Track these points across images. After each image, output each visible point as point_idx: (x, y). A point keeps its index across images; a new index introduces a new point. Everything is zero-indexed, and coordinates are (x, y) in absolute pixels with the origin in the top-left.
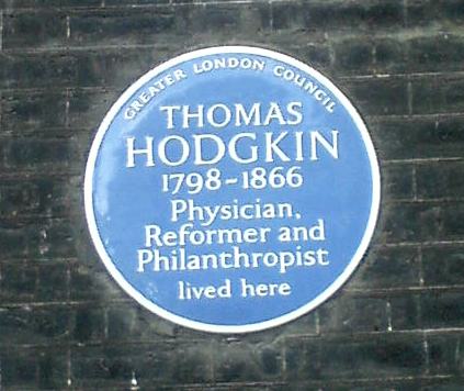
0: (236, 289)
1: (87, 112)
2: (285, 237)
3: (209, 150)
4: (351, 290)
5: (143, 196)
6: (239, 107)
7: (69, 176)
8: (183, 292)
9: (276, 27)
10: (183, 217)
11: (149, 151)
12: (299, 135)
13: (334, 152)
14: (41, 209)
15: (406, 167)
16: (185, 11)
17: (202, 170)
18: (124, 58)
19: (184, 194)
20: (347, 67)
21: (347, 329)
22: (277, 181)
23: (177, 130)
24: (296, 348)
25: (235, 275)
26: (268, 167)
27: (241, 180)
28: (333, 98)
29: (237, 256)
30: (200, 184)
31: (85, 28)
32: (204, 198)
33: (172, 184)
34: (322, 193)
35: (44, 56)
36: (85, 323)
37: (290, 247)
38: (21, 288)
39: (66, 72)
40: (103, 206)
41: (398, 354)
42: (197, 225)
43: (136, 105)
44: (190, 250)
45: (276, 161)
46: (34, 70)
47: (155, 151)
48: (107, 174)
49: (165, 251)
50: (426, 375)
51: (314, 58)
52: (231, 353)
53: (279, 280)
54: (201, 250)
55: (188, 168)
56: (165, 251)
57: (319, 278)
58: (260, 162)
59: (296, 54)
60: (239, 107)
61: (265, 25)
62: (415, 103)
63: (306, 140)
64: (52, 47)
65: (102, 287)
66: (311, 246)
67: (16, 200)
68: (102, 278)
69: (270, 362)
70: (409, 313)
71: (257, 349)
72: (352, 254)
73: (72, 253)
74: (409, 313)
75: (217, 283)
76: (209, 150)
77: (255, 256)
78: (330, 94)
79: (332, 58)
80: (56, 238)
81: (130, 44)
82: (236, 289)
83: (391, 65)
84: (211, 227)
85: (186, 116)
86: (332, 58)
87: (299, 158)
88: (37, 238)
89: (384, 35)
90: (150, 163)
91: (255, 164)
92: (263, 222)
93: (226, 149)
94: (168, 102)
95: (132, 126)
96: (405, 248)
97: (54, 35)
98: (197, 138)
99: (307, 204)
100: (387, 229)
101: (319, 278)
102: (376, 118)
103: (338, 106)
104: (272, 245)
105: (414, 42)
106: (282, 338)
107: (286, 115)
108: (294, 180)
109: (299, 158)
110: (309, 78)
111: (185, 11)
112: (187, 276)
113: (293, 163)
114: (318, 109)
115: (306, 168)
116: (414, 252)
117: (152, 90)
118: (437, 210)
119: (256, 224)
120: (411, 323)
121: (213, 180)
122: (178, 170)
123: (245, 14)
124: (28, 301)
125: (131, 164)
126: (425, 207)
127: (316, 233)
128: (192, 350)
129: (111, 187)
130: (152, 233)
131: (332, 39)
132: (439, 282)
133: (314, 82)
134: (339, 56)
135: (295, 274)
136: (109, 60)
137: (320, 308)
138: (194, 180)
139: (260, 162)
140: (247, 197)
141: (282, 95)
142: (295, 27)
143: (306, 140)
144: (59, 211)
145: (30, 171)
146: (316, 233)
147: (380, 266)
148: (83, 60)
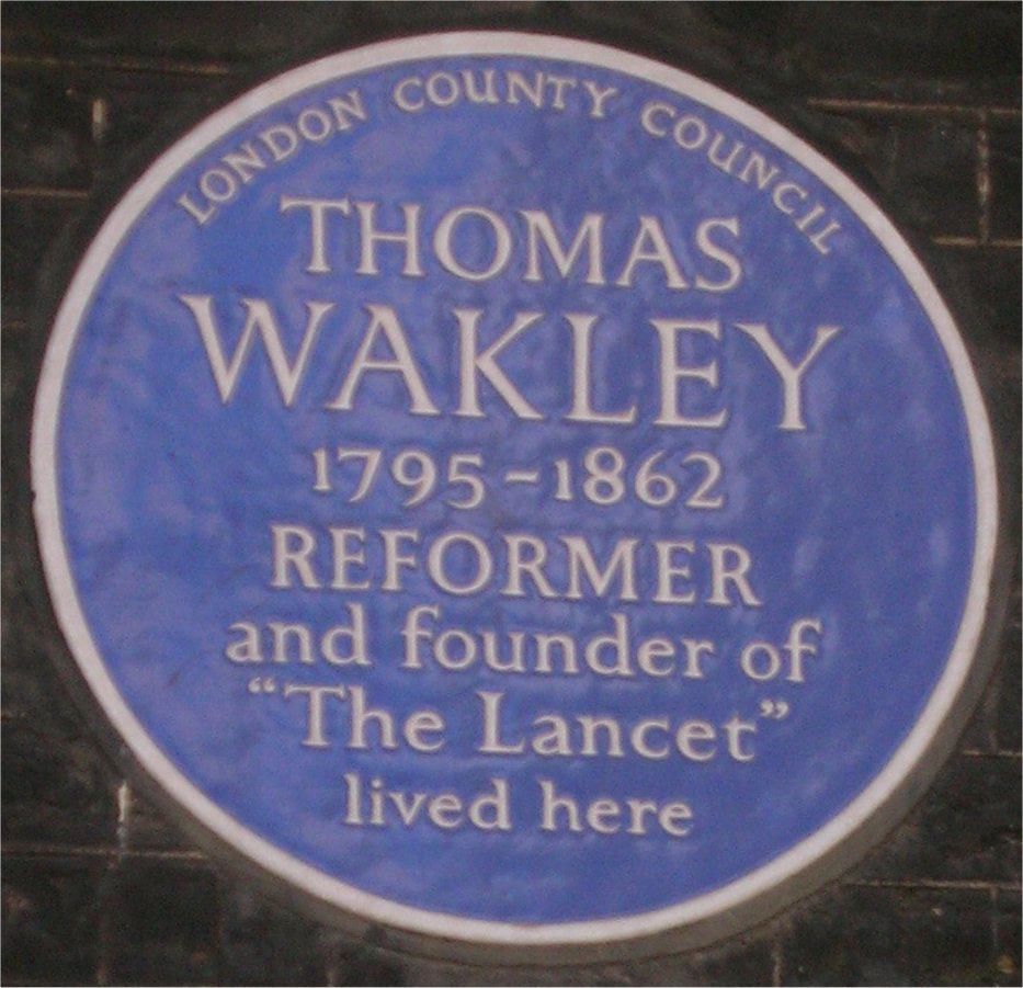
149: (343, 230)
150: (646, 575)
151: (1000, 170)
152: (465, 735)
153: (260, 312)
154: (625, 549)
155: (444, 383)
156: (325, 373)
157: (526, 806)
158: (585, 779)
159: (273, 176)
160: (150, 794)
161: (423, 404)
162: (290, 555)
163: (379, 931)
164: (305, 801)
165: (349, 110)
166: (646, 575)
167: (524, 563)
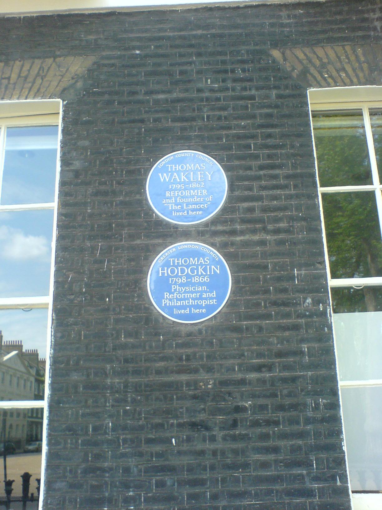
0: (190, 310)
1: (148, 260)
2: (204, 296)
3: (183, 271)
4: (223, 311)
5: (164, 284)
6: (191, 259)
7: (143, 278)
8: (175, 312)
9: (202, 236)
10: (175, 290)
11: (166, 271)
12: (208, 267)
13: (218, 272)
14: (135, 288)
15: (239, 276)
16: (176, 231)
17: (181, 277)
18: (159, 245)
19: (176, 283)
20: (222, 247)
21: (222, 322)
22: (202, 280)
23: (174, 265)
24: (207, 327)
25: (190, 307)
26: (200, 276)
27: (192, 280)
28: (218, 256)
29: (191, 301)
30: (180, 281)
31: (147, 236)
32: (181, 285)
33: (172, 281)
34: (215, 283)
35: (136, 244)
36: (148, 320)
37: (206, 299)
38: (129, 310)
39: (142, 249)
40: (153, 287)
41: (236, 329)
42: (179, 293)
43: (162, 258)
44: (177, 299)
45: (202, 274)
46: (133, 248)
47: (167, 272)
48: (154, 278)
49: (170, 300)
50: (244, 335)
51: (213, 245)
52: (189, 329)
53: (203, 308)
54: (181, 300)
55: (177, 276)
56: (170, 300)
57: (214, 307)
58: (197, 274)
59: (207, 244)
60: (191, 259)
61: (199, 235)
62: (241, 258)
63: (210, 268)
64: (138, 242)
65: (152, 310)
66: (212, 298)
67: (128, 285)
68: (152, 307)
69: (200, 332)
70: (240, 317)
71: (196, 328)
72: (224, 300)
73: (144, 300)
74: (240, 317)
75: (185, 309)
76: (183, 271)
77: (196, 301)
78: (217, 255)
79: (218, 245)
80: (139, 296)
81: (160, 241)
82: (190, 310)
83: (235, 247)
84: (183, 293)
85: (176, 261)
86: (218, 245)
87: (208, 273)
88: (134, 296)
89: (232, 238)
90: (166, 275)
91: (196, 275)
92: (198, 292)
93: (188, 271)
94: (171, 258)
95: (161, 264)
96: (239, 299)
97: (139, 239)
98: (179, 268)
99: (211, 287)
100: (233, 294)
101: (214, 307)
102: (231, 262)
103: (220, 259)
104: (201, 298)
105: (241, 240)
106: (203, 325)
107: (205, 261)
108: (207, 280)
109: (208, 273)
110: (211, 251)
111: (176, 231)
112: (177, 307)
113: (207, 275)
114: (214, 259)
115: (210, 276)
116: (241, 300)
117: (167, 254)
118: (248, 288)
119: (196, 292)
120: (240, 320)
121: (184, 280)
122: (174, 277)
123: (193, 232)
124: (131, 314)
125: (160, 275)
126: (244, 287)
127: (213, 295)
128: (178, 328)
129: (155, 282)
130: (166, 295)
131: (218, 240)
132: (248, 309)
133: (213, 252)
134: (220, 244)
135: (207, 306)
136: (154, 246)
137: (214, 316)
138: (178, 280)
139: (197, 274)
140: (194, 284)
141: (203, 256)
142: (207, 236)
143: (210, 268)
144: (140, 289)
145: (132, 277)
146: (213, 295)
147: (231, 304)
148: (147, 246)
149: (172, 168)
150: (197, 193)
151: (226, 158)
152: (182, 208)
153: (165, 174)
154: (196, 191)
155: (180, 179)
156: (170, 180)
157: (188, 213)
158: (193, 210)
159: (166, 164)
160: (156, 215)
161: (179, 180)
162: (168, 194)
163: (176, 224)
164: (169, 214)
165: (172, 158)
166: (197, 193)
167: (187, 193)
